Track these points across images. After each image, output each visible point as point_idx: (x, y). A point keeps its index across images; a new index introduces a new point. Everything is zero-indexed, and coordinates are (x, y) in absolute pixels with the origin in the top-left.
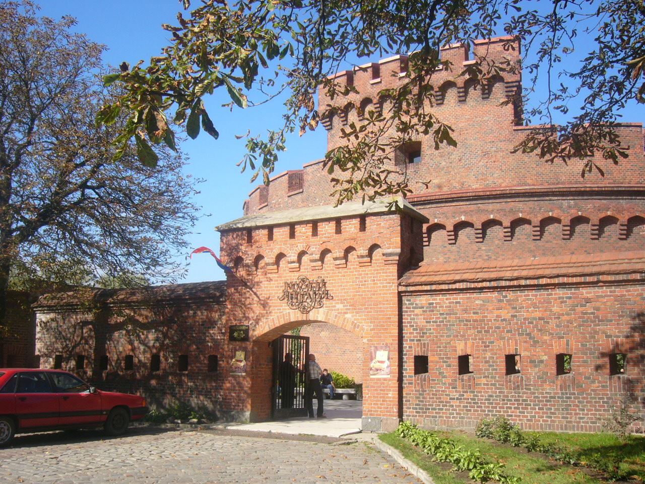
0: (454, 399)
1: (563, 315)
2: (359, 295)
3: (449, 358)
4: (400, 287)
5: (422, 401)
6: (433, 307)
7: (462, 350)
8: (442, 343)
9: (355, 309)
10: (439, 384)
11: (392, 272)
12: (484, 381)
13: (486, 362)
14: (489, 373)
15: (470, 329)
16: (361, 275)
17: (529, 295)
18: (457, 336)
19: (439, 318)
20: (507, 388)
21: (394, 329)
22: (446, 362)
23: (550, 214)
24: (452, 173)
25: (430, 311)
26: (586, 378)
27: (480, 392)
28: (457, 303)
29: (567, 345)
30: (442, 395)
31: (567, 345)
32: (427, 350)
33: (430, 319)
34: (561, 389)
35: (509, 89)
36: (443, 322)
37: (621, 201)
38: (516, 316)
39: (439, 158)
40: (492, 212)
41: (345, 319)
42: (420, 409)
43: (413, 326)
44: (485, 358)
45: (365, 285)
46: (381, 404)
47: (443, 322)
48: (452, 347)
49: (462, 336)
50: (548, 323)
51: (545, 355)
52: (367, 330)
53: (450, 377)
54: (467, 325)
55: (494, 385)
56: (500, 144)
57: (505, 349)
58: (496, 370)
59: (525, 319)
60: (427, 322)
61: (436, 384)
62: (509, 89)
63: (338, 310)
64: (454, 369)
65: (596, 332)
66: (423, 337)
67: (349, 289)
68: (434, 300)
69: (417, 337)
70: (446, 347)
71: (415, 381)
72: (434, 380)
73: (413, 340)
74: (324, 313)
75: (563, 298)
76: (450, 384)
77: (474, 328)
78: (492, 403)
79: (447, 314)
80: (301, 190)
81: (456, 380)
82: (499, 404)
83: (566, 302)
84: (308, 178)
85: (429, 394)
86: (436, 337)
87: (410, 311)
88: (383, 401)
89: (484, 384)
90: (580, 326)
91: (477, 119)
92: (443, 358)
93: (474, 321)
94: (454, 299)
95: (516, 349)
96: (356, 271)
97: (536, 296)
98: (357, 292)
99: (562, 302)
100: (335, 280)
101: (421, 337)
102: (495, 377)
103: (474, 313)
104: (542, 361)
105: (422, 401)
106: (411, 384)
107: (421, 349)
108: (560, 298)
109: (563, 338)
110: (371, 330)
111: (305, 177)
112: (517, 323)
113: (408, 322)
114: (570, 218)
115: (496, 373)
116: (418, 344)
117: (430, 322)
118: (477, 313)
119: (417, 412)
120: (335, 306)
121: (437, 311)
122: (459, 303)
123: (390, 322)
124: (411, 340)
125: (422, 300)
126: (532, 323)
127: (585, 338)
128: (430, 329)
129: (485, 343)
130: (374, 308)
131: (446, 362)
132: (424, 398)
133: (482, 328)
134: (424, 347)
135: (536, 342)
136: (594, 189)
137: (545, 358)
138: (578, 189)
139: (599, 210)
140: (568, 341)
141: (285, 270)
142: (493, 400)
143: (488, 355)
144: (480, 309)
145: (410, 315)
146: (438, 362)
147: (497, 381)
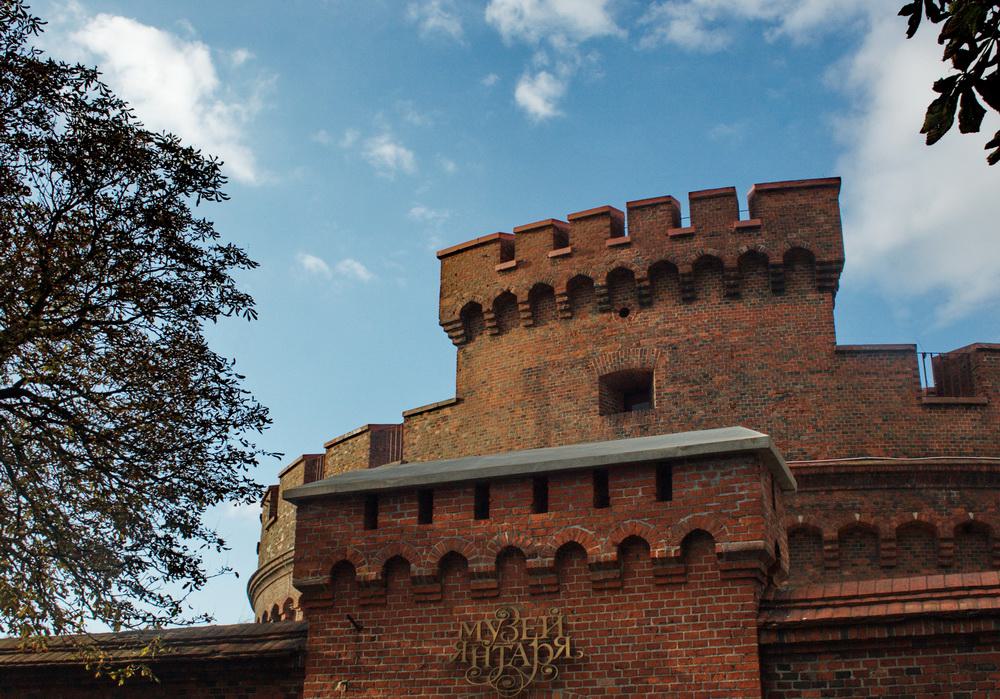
2: (657, 655)
11: (743, 599)
16: (661, 604)
28: (910, 671)
40: (801, 510)
62: (823, 276)
67: (631, 640)
68: (852, 665)
94: (901, 662)
98: (650, 647)
120: (593, 683)
122: (916, 671)
138: (966, 469)
141: (462, 595)
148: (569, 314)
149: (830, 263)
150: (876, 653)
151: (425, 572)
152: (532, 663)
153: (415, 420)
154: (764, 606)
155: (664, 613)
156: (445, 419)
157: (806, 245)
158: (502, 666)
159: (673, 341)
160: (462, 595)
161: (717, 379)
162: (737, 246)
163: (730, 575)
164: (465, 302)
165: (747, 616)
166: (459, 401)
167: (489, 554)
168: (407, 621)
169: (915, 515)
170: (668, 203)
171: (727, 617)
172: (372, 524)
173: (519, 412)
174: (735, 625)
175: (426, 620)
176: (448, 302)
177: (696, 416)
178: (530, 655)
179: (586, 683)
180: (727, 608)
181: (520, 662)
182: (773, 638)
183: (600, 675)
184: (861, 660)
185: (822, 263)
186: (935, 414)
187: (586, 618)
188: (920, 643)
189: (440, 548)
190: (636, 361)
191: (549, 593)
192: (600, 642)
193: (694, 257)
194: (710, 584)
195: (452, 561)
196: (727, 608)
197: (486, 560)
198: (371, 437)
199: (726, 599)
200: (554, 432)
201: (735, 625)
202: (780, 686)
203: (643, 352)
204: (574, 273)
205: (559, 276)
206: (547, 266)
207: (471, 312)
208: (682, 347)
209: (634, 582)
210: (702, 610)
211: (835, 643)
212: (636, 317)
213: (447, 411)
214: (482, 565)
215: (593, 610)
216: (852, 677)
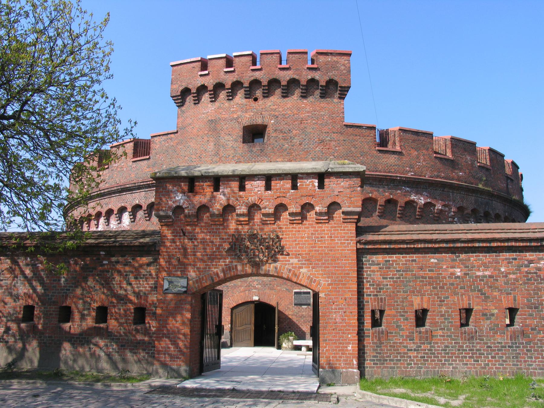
0: (411, 350)
2: (315, 251)
3: (406, 312)
5: (380, 353)
6: (389, 264)
7: (419, 305)
9: (311, 264)
10: (397, 336)
11: (351, 230)
12: (440, 333)
13: (442, 315)
14: (445, 326)
15: (426, 285)
16: (317, 231)
18: (414, 292)
19: (395, 274)
20: (462, 339)
21: (353, 284)
23: (370, 195)
26: (532, 329)
27: (437, 343)
28: (413, 261)
29: (515, 300)
30: (400, 347)
31: (515, 300)
32: (385, 304)
33: (387, 275)
34: (511, 339)
41: (300, 273)
42: (377, 360)
43: (369, 281)
44: (441, 311)
45: (322, 241)
47: (399, 278)
48: (409, 301)
50: (497, 280)
51: (496, 309)
52: (324, 284)
55: (450, 336)
58: (452, 322)
60: (383, 278)
61: (394, 336)
63: (292, 264)
64: (411, 322)
66: (380, 292)
67: (304, 244)
68: (391, 257)
69: (374, 292)
70: (403, 302)
73: (370, 295)
75: (509, 259)
76: (407, 336)
77: (430, 284)
78: (448, 353)
79: (403, 271)
80: (148, 157)
81: (413, 333)
82: (455, 353)
84: (155, 146)
85: (386, 346)
89: (440, 336)
90: (525, 283)
91: (315, 113)
92: (400, 312)
93: (429, 278)
95: (469, 304)
96: (312, 227)
98: (312, 247)
99: (508, 263)
100: (289, 234)
103: (429, 271)
104: (493, 315)
105: (380, 353)
107: (378, 303)
108: (506, 259)
109: (511, 294)
110: (329, 285)
111: (152, 145)
114: (384, 199)
115: (451, 326)
116: (375, 299)
117: (387, 278)
118: (432, 271)
119: (374, 364)
121: (394, 268)
122: (415, 261)
125: (379, 258)
126: (483, 280)
127: (530, 294)
128: (387, 285)
129: (441, 298)
130: (332, 264)
133: (437, 284)
134: (381, 302)
135: (487, 298)
137: (496, 311)
140: (515, 297)
142: (449, 350)
143: (444, 309)
146: (395, 316)
147: (453, 333)
148: (231, 98)
149: (345, 87)
153: (156, 139)
156: (171, 139)
157: (336, 78)
159: (277, 113)
161: (294, 132)
162: (307, 75)
163: (346, 221)
164: (183, 87)
165: (352, 237)
166: (177, 132)
169: (370, 195)
170: (278, 53)
171: (344, 237)
173: (206, 138)
176: (174, 87)
177: (284, 147)
180: (344, 233)
182: (362, 246)
184: (395, 256)
190: (259, 121)
191: (270, 224)
192: (292, 245)
193: (288, 78)
196: (344, 233)
198: (134, 144)
199: (344, 230)
200: (222, 149)
203: (263, 117)
204: (235, 80)
205: (229, 80)
206: (218, 74)
207: (186, 92)
212: (261, 102)
213: (173, 136)
215: (289, 231)
216: (391, 262)
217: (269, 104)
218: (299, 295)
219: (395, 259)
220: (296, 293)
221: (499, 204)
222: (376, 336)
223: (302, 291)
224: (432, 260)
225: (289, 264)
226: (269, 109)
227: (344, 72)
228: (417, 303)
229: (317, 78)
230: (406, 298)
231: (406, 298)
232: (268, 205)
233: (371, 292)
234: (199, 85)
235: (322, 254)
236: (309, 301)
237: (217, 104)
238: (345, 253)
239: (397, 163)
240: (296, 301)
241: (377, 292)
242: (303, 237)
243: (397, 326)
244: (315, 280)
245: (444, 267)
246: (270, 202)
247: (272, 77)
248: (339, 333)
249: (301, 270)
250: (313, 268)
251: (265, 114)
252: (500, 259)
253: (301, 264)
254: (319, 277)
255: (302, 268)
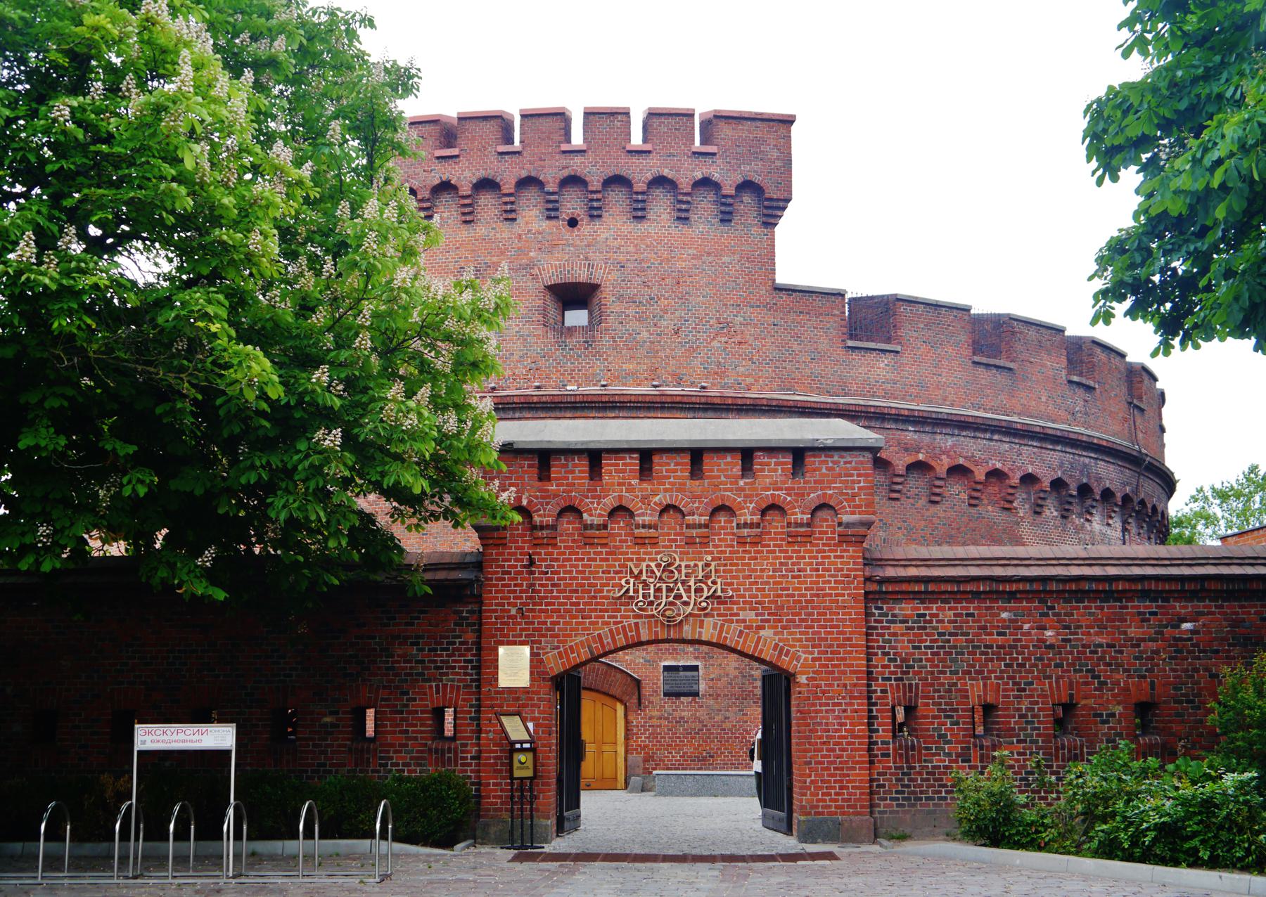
1: (1144, 640)
2: (788, 595)
4: (868, 583)
5: (909, 786)
6: (925, 622)
7: (979, 696)
8: (943, 684)
9: (780, 621)
15: (992, 660)
16: (791, 558)
17: (1090, 608)
18: (970, 672)
19: (936, 641)
22: (952, 717)
24: (661, 354)
25: (919, 628)
28: (968, 615)
29: (1153, 689)
32: (917, 695)
35: (770, 212)
36: (943, 647)
37: (938, 437)
38: (1069, 640)
39: (634, 325)
41: (759, 638)
42: (904, 799)
43: (888, 654)
45: (799, 577)
46: (836, 794)
47: (943, 647)
48: (960, 690)
49: (977, 672)
50: (1121, 652)
51: (1119, 703)
52: (806, 659)
53: (958, 742)
54: (987, 653)
56: (749, 310)
57: (1052, 696)
58: (1038, 729)
59: (1083, 646)
60: (914, 647)
61: (934, 755)
63: (744, 621)
65: (1197, 670)
67: (768, 583)
69: (895, 673)
70: (949, 691)
71: (895, 749)
72: (927, 749)
74: (715, 628)
75: (1144, 613)
76: (958, 755)
77: (999, 659)
79: (951, 634)
83: (1148, 620)
85: (920, 774)
86: (932, 673)
87: (883, 628)
88: (841, 788)
91: (710, 259)
92: (944, 711)
93: (998, 647)
94: (962, 608)
96: (780, 551)
97: (1102, 608)
98: (782, 589)
99: (1143, 620)
100: (737, 565)
101: (903, 673)
102: (1037, 742)
103: (999, 634)
105: (909, 786)
106: (888, 755)
108: (1139, 614)
110: (814, 659)
112: (1071, 653)
113: (879, 647)
115: (1038, 735)
116: (898, 686)
117: (919, 648)
118: (1003, 634)
119: (898, 805)
120: (738, 615)
121: (934, 628)
123: (851, 646)
124: (884, 679)
125: (904, 609)
126: (1096, 652)
128: (921, 660)
129: (1019, 684)
131: (952, 717)
132: (910, 780)
134: (911, 691)
136: (902, 412)
137: (1118, 709)
139: (906, 450)
141: (626, 541)
144: (1008, 627)
145: (883, 635)
146: (934, 717)
147: (1041, 748)
149: (778, 200)
150: (945, 601)
151: (596, 521)
152: (689, 597)
154: (869, 562)
155: (793, 564)
157: (757, 179)
158: (664, 600)
160: (626, 541)
161: (663, 303)
167: (653, 509)
168: (577, 560)
171: (842, 570)
172: (544, 476)
174: (848, 576)
175: (595, 560)
178: (688, 591)
179: (732, 615)
181: (679, 597)
183: (744, 609)
185: (771, 199)
186: (856, 356)
187: (731, 565)
188: (977, 595)
189: (610, 501)
190: (582, 275)
192: (743, 584)
193: (649, 176)
194: (829, 545)
195: (620, 510)
197: (651, 515)
199: (842, 557)
201: (848, 576)
202: (876, 621)
204: (524, 174)
208: (630, 266)
209: (770, 540)
210: (823, 563)
211: (920, 592)
212: (586, 228)
214: (647, 518)
215: (737, 558)
217: (604, 236)
218: (673, 674)
219: (935, 611)
220: (667, 668)
221: (1112, 467)
222: (901, 755)
223: (681, 663)
224: (1004, 615)
225: (738, 621)
226: (605, 246)
227: (779, 164)
228: (976, 691)
229: (716, 176)
230: (955, 684)
231: (955, 684)
232: (698, 508)
233: (891, 673)
234: (437, 182)
235: (800, 602)
236: (695, 687)
237: (481, 230)
238: (844, 601)
239: (890, 376)
240: (667, 687)
241: (903, 673)
242: (763, 571)
243: (940, 736)
244: (788, 651)
245: (1026, 626)
246: (700, 503)
247: (611, 171)
248: (834, 750)
249: (762, 633)
250: (784, 628)
251: (597, 258)
252: (1127, 614)
253: (762, 621)
254: (794, 646)
255: (763, 628)
